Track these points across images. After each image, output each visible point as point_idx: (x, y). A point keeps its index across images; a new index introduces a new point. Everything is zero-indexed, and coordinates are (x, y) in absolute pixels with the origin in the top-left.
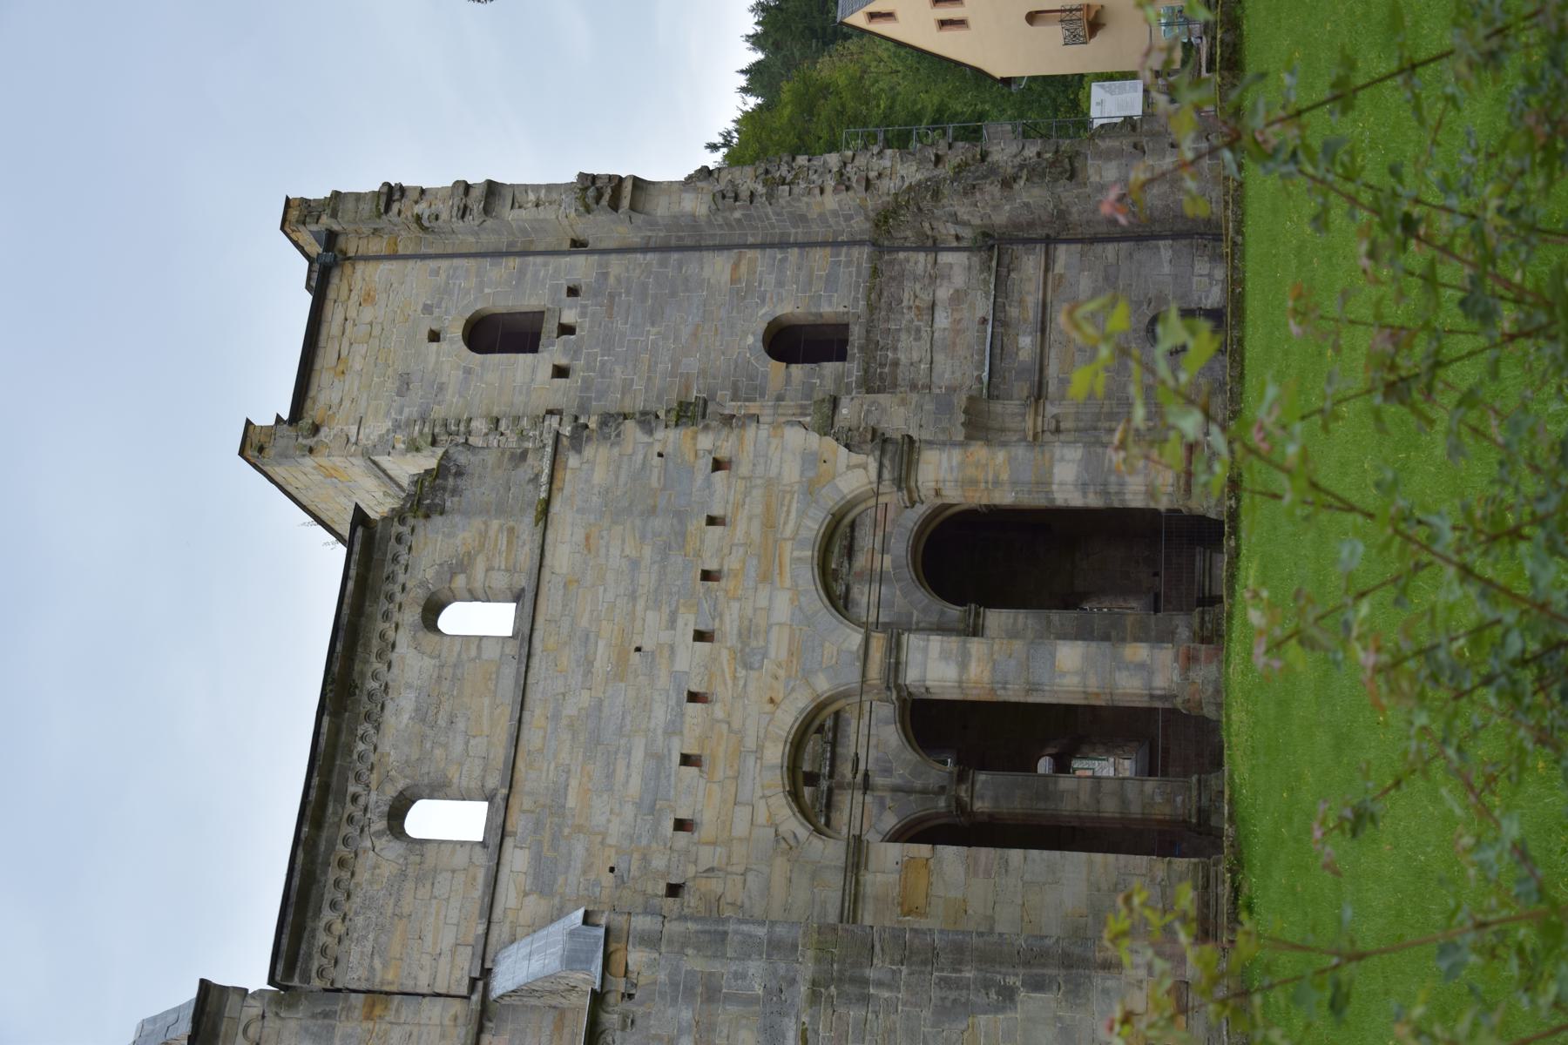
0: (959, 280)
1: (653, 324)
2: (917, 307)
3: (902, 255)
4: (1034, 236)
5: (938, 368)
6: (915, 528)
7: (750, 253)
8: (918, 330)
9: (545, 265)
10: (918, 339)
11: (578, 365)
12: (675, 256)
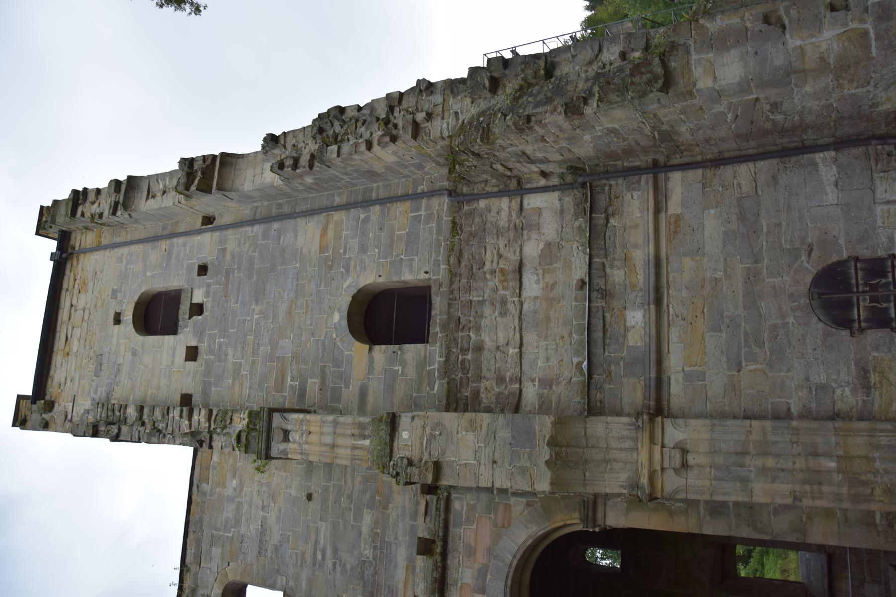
0: (550, 229)
1: (257, 304)
2: (502, 271)
3: (482, 203)
4: (637, 163)
5: (528, 350)
6: (515, 563)
7: (337, 216)
8: (504, 302)
9: (185, 245)
10: (504, 313)
11: (203, 347)
12: (276, 225)
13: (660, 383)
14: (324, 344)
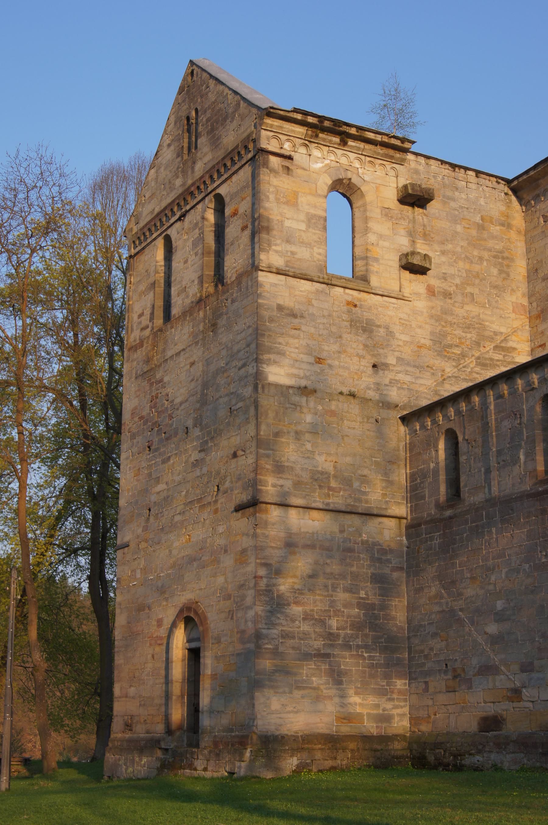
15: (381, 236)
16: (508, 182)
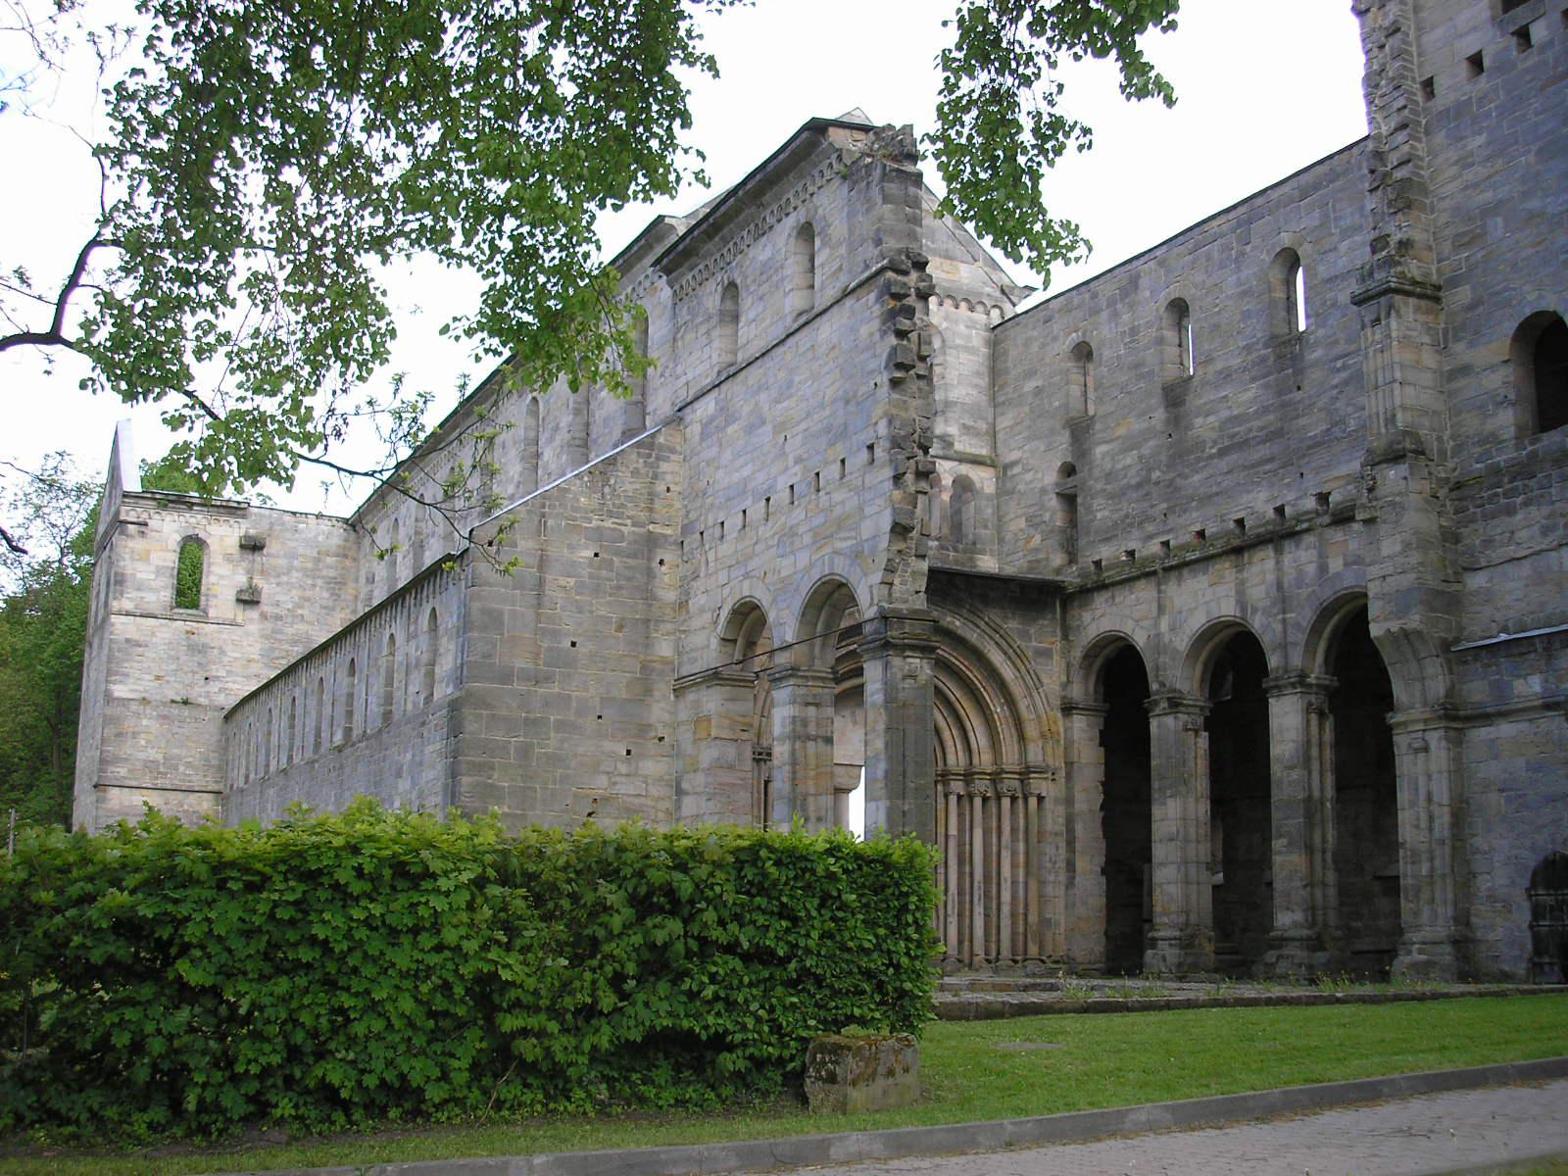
13: (1485, 718)
14: (1506, 289)
15: (222, 577)
16: (346, 521)
